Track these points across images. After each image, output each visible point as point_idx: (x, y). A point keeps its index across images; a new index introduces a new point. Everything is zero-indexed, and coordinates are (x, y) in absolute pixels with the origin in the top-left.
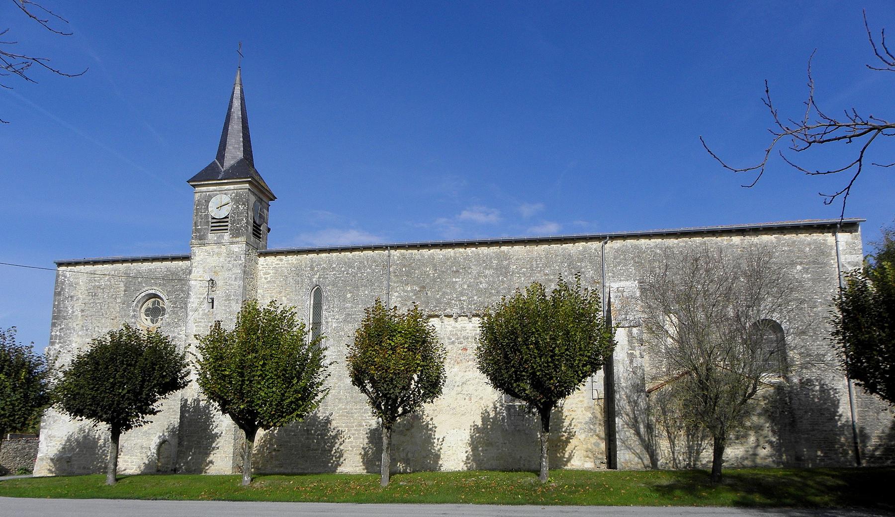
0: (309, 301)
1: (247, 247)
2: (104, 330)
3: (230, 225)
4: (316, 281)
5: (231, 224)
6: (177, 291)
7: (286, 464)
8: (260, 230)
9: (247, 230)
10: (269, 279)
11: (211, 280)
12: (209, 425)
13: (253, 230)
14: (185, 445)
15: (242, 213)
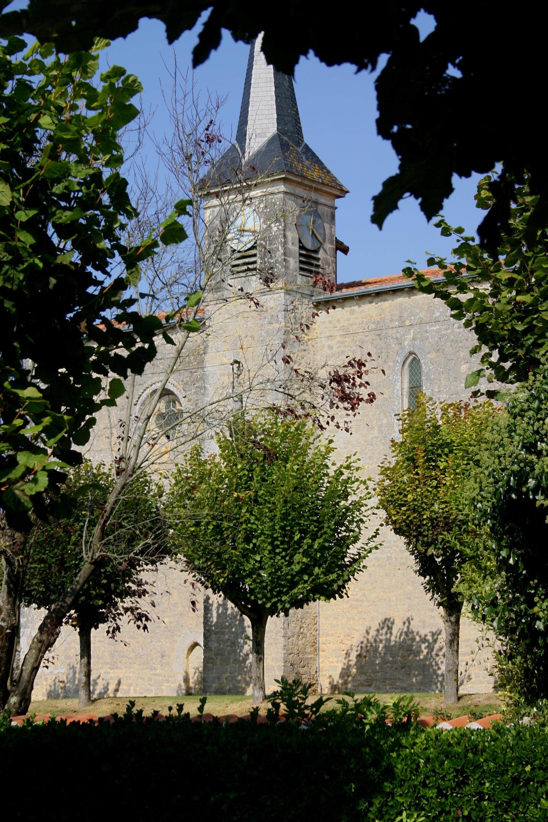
0: (399, 384)
1: (288, 297)
2: (97, 457)
3: (259, 261)
4: (410, 346)
5: (261, 258)
6: (198, 381)
7: (377, 680)
8: (318, 259)
9: (286, 267)
10: (335, 349)
11: (236, 362)
12: (343, 543)
13: (301, 262)
14: (213, 649)
15: (276, 237)
